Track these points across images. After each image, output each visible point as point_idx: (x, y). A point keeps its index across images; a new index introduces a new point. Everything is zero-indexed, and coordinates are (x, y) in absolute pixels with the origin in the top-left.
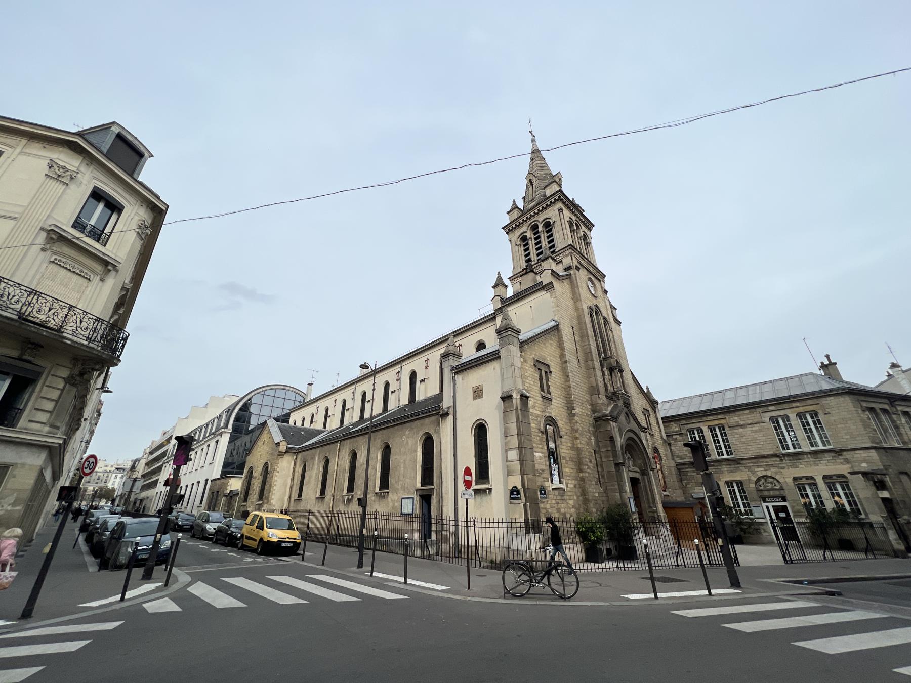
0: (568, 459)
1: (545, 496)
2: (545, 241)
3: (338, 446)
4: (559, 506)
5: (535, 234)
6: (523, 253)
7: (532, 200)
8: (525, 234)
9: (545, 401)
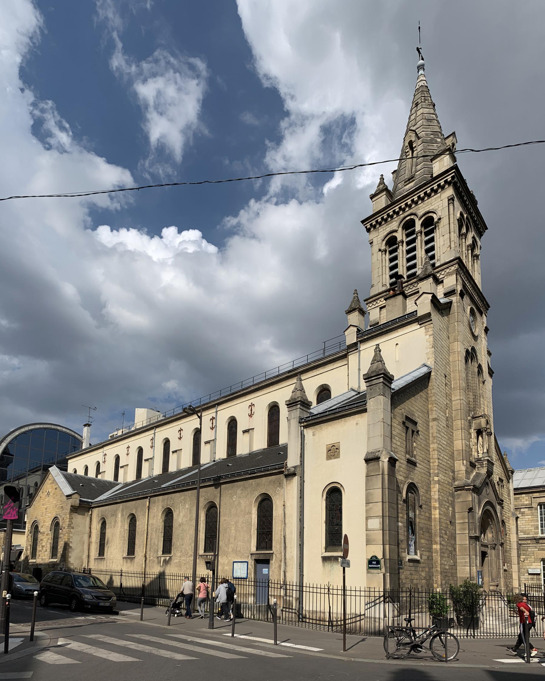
2: (421, 248)
3: (148, 503)
5: (408, 235)
6: (388, 265)
7: (411, 179)
8: (394, 234)
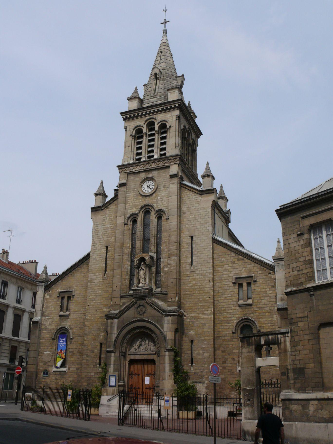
0: (75, 352)
1: (47, 375)
4: (58, 381)
9: (63, 318)
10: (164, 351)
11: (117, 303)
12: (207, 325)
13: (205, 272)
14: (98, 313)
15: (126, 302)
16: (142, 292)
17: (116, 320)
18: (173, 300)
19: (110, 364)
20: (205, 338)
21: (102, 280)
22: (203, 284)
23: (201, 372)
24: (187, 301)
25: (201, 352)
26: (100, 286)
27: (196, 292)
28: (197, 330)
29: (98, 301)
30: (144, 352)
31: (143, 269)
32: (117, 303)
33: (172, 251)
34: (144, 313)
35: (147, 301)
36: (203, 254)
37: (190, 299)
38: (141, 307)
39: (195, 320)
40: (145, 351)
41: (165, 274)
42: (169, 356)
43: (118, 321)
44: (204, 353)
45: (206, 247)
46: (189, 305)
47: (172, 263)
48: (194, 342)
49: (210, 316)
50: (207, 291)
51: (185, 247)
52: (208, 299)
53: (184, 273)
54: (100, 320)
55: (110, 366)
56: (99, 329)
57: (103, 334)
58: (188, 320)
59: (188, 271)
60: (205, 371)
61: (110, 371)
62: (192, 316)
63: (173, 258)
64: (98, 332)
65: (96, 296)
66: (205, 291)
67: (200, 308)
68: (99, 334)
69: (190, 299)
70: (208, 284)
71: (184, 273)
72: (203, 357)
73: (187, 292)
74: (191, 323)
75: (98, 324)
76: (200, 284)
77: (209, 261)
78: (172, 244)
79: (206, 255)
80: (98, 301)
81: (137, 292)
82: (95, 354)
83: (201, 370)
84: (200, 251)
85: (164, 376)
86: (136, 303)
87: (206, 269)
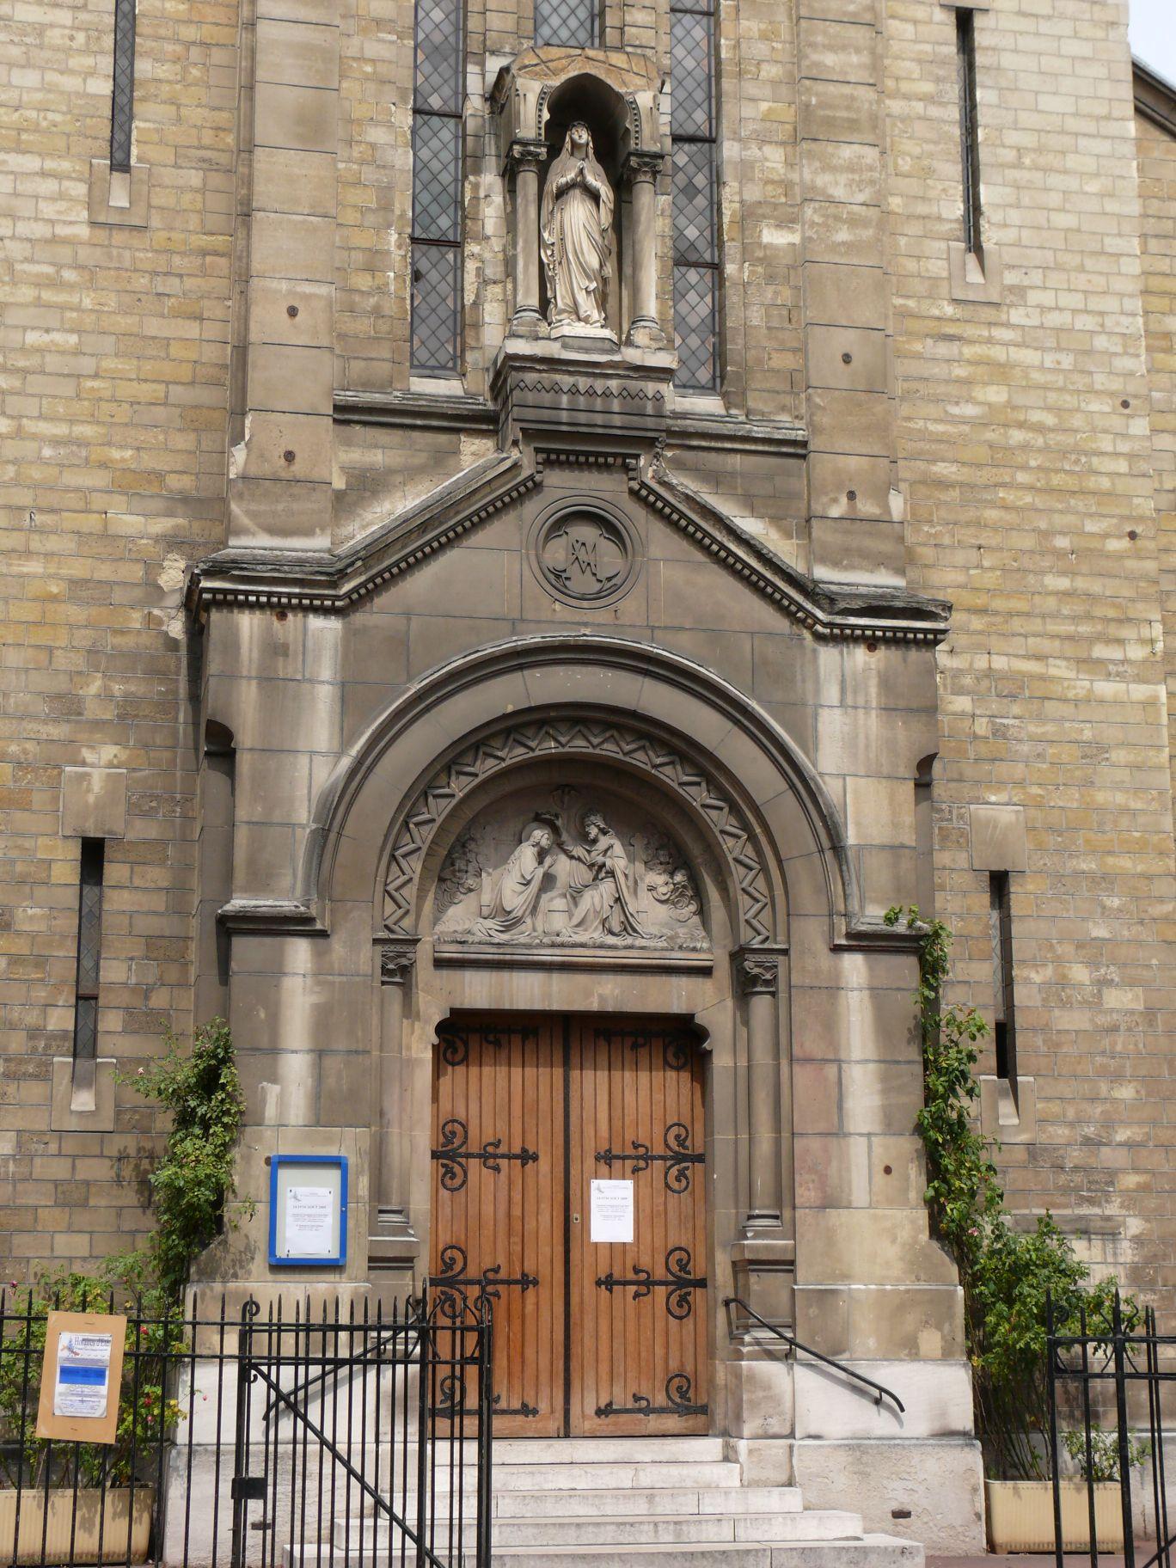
10: (822, 947)
11: (299, 468)
12: (1120, 756)
13: (1086, 322)
14: (53, 544)
15: (391, 471)
16: (607, 394)
17: (325, 628)
18: (866, 507)
19: (274, 1051)
20: (1110, 860)
21: (84, 231)
22: (1077, 421)
23: (1088, 1142)
24: (947, 541)
25: (1080, 974)
26: (71, 287)
27: (1022, 477)
28: (1035, 790)
29: (44, 428)
30: (602, 946)
31: (595, 197)
32: (299, 468)
33: (831, 88)
34: (608, 589)
35: (648, 476)
36: (1065, 172)
37: (968, 524)
38: (586, 532)
39: (1016, 709)
40: (611, 940)
41: (770, 278)
42: (874, 991)
43: (349, 635)
44: (1103, 983)
45: (1090, 127)
46: (960, 578)
47: (839, 193)
48: (1019, 893)
49: (1140, 691)
50: (1105, 483)
51: (905, 87)
52: (1117, 545)
53: (911, 303)
54: (75, 613)
55: (275, 1061)
56: (67, 706)
57: (109, 752)
58: (962, 703)
59: (944, 291)
60: (1122, 1135)
61: (270, 1112)
62: (989, 673)
63: (847, 152)
64: (57, 731)
65: (25, 372)
66: (1092, 483)
67: (1055, 616)
68: (69, 751)
69: (968, 524)
70: (1117, 422)
71: (911, 303)
72: (1102, 1020)
73: (942, 469)
74: (981, 727)
75: (50, 650)
76: (1050, 420)
77: (1112, 244)
78: (834, 28)
79: (1093, 187)
80: (44, 428)
81: (556, 389)
82: (21, 947)
83: (1090, 1131)
84: (1039, 150)
85: (833, 1170)
86: (533, 487)
87: (1095, 303)
